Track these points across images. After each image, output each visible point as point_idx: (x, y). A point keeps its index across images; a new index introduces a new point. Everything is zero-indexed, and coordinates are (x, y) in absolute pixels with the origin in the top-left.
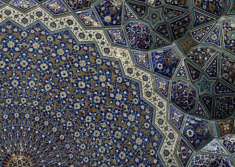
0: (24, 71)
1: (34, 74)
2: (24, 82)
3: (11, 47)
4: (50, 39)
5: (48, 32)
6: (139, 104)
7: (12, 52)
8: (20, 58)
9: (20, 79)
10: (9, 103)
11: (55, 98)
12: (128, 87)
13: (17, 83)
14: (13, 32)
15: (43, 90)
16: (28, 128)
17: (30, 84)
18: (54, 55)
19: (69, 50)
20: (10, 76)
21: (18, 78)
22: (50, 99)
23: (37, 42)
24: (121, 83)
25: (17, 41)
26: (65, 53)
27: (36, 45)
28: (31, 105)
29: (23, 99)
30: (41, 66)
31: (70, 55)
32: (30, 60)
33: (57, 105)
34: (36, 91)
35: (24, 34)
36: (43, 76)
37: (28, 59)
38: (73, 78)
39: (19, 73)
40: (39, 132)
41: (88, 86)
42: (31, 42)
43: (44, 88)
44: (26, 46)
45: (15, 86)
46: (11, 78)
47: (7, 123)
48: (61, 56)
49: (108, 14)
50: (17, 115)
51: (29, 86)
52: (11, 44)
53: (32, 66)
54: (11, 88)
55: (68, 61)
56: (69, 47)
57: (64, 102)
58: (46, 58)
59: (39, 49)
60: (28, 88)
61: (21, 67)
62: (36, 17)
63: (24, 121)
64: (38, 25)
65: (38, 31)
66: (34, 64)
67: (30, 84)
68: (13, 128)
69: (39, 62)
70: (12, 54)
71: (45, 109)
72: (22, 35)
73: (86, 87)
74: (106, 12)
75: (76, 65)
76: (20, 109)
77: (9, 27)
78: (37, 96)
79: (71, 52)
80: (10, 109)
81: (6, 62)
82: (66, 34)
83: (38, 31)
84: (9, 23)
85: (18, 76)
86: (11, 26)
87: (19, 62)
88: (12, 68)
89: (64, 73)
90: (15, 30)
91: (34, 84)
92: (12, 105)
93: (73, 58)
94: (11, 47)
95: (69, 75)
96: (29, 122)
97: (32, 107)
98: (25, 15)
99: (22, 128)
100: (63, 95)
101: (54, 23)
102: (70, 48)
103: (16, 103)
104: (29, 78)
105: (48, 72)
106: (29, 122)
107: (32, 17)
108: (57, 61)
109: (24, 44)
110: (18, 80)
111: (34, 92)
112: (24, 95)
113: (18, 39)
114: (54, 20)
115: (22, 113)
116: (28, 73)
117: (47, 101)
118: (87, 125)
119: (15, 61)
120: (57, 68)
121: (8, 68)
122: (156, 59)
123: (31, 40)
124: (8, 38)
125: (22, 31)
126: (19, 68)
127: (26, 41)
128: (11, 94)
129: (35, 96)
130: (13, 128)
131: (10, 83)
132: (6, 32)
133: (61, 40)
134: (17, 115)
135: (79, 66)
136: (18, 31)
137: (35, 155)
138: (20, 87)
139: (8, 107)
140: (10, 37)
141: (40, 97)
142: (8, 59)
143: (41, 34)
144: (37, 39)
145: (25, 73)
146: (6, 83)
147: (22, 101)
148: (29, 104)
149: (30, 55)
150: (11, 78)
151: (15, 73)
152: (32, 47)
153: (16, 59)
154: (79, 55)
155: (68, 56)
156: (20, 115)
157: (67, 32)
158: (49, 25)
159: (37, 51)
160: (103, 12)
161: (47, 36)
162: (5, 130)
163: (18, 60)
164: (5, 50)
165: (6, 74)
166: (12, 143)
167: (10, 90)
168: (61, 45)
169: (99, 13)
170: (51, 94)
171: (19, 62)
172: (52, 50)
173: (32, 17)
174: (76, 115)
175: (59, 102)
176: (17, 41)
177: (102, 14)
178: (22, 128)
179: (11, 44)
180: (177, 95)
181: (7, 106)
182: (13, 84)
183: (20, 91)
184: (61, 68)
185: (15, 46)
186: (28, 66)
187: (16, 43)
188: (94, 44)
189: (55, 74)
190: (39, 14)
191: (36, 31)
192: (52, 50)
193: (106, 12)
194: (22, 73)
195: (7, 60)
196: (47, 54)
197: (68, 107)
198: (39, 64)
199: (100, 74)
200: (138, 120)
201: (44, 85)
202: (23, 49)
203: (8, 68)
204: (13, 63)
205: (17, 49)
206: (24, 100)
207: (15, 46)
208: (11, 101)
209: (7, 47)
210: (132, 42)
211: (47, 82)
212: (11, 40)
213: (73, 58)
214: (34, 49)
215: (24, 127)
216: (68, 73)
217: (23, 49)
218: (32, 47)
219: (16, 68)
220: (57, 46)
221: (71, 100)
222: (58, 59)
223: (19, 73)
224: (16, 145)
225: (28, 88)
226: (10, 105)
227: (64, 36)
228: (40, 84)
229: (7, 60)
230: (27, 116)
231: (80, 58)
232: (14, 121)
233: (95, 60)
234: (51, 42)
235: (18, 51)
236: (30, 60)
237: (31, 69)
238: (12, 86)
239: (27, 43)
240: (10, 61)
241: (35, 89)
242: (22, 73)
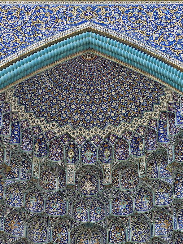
0: (83, 103)
1: (78, 102)
2: (83, 98)
3: (88, 116)
4: (69, 121)
5: (70, 124)
6: (25, 103)
7: (88, 114)
8: (85, 110)
9: (86, 99)
10: (92, 87)
11: (68, 91)
12: (32, 108)
13: (87, 97)
14: (86, 124)
15: (74, 94)
16: (83, 74)
17: (81, 97)
18: (68, 113)
19: (60, 117)
20: (90, 101)
21: (86, 100)
22: (71, 90)
23: (76, 119)
24: (35, 108)
25: (85, 119)
26: (62, 115)
27: (76, 117)
28: (81, 86)
29: (85, 89)
30: (74, 106)
31: (60, 115)
32: (80, 109)
33: (67, 88)
34: (78, 94)
35: (81, 123)
36: (74, 102)
37: (80, 110)
38: (58, 103)
39: (86, 103)
40: (78, 72)
41: (51, 101)
42: (79, 119)
43: (74, 95)
44: (81, 116)
45: (88, 96)
46: (90, 100)
47: (94, 77)
48: (64, 113)
49: (41, 138)
50: (89, 80)
51: (81, 96)
52: (88, 118)
53: (79, 106)
54: (90, 95)
55: (61, 111)
56: (60, 119)
57: (64, 90)
58: (72, 111)
59: (75, 116)
60: (82, 95)
61: (84, 106)
62: (75, 132)
63: (85, 77)
64: (75, 128)
65: (75, 125)
66: (78, 107)
67: (81, 97)
68: (91, 74)
69: (75, 109)
70: (88, 113)
71: (74, 85)
72: (82, 122)
73: (52, 100)
74: (42, 140)
75: (57, 110)
76: (87, 84)
77: (88, 126)
78: (77, 91)
79: (59, 116)
80: (92, 84)
81: (91, 108)
82: (61, 125)
83: (75, 125)
84: (88, 129)
85: (86, 101)
86: (87, 127)
87: (85, 108)
88: (89, 105)
89: (63, 104)
90: (85, 125)
91: (79, 97)
92: (90, 86)
93: (58, 113)
94: (88, 116)
95: (60, 104)
96: (83, 77)
97: (80, 85)
98: (80, 132)
99: (86, 74)
100: (64, 94)
101: (67, 129)
102: (59, 118)
103: (88, 87)
104: (81, 100)
105: (71, 104)
106: (83, 77)
107: (77, 132)
108: (66, 110)
109: (82, 118)
110: (87, 99)
111: (79, 93)
112: (84, 91)
113: (84, 120)
114: (66, 131)
115: (86, 82)
116: (81, 102)
117: (72, 89)
118: (52, 83)
119: (87, 109)
120: (66, 107)
121: (91, 105)
122: (18, 127)
123: (79, 120)
124: (89, 121)
125: (82, 124)
126: (85, 105)
127: (81, 119)
128: (91, 92)
129: (79, 91)
130: (91, 74)
131: (90, 98)
132: (90, 124)
133: (64, 121)
134: (89, 80)
135: (55, 110)
136: (84, 125)
137: (81, 60)
138: (86, 95)
139: (93, 85)
140: (88, 121)
141: (76, 91)
142: (90, 110)
143: (74, 123)
144: (75, 121)
145: (82, 103)
146: (93, 97)
147: (85, 88)
148: (82, 86)
149: (79, 112)
150: (90, 100)
151: (87, 103)
152: (78, 116)
153: (86, 110)
154: (56, 115)
155: (61, 114)
156: (87, 81)
157: (61, 125)
158: (69, 128)
159: (76, 114)
160: (43, 140)
161: (70, 122)
162: (95, 73)
163: (85, 109)
164: (91, 115)
165: (92, 102)
166: (92, 66)
167: (91, 94)
168: (64, 118)
169: (45, 140)
170: (70, 93)
171: (85, 108)
172: (69, 115)
173: (77, 132)
174: (58, 86)
175: (66, 90)
176: (85, 119)
177: (44, 139)
178: (86, 74)
179: (88, 118)
180: (7, 116)
181: (93, 86)
182: (89, 97)
183: (86, 93)
184: (65, 107)
185: (86, 116)
186: (81, 106)
187: (86, 118)
188: (48, 122)
189: (68, 103)
190: (73, 134)
191: (76, 125)
192: (69, 115)
193: (42, 140)
194: (84, 103)
195: (91, 110)
196: (71, 113)
197: (62, 88)
198: (75, 107)
199: (45, 109)
200: (26, 96)
201: (74, 97)
202: (82, 115)
203: (91, 105)
204: (88, 108)
205: (86, 115)
206: (84, 88)
207: (86, 116)
208: (91, 88)
209: (90, 116)
210: (29, 130)
211: (72, 99)
212: (88, 120)
213: (58, 113)
214: (77, 115)
215: (85, 74)
216: (61, 105)
217: (82, 115)
218: (78, 116)
219: (87, 105)
220: (66, 118)
221: (60, 92)
222: (66, 111)
223: (86, 103)
224: (90, 65)
225: (82, 95)
226: (92, 86)
227: (62, 124)
228: (76, 97)
229: (91, 110)
230: (83, 80)
231: (55, 114)
232: (90, 78)
233: (47, 115)
234: (69, 119)
235: (85, 114)
236: (80, 109)
237: (79, 105)
238: (90, 96)
239: (80, 118)
240: (89, 109)
241: (78, 95)
242: (84, 103)
